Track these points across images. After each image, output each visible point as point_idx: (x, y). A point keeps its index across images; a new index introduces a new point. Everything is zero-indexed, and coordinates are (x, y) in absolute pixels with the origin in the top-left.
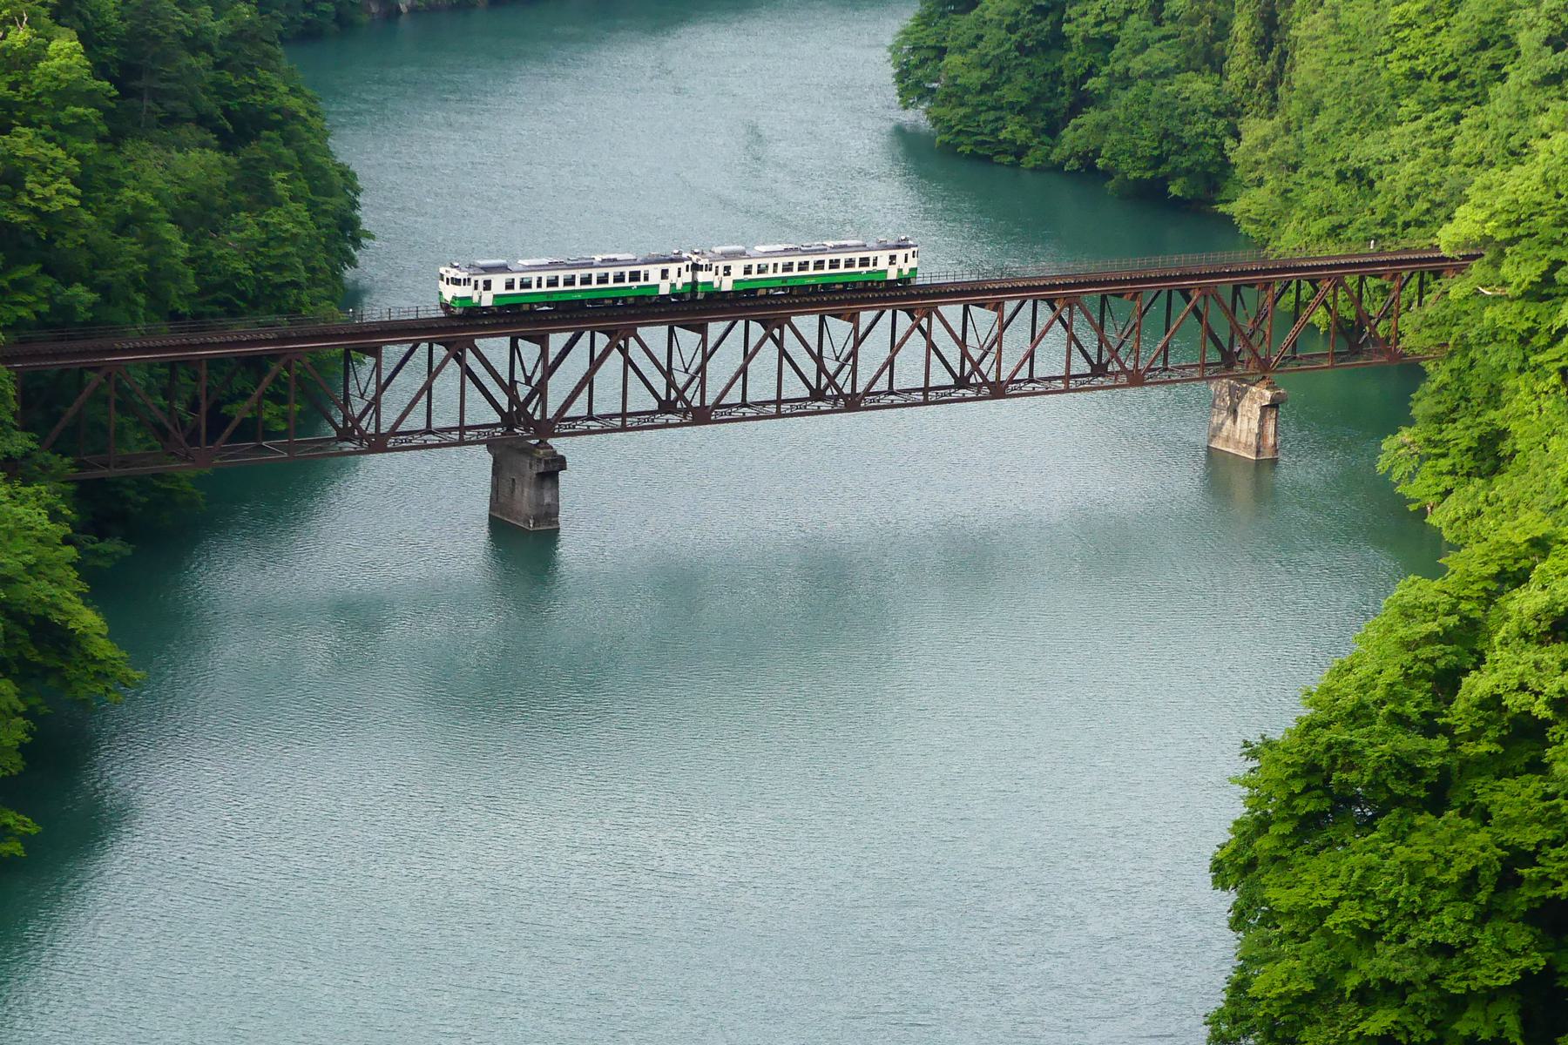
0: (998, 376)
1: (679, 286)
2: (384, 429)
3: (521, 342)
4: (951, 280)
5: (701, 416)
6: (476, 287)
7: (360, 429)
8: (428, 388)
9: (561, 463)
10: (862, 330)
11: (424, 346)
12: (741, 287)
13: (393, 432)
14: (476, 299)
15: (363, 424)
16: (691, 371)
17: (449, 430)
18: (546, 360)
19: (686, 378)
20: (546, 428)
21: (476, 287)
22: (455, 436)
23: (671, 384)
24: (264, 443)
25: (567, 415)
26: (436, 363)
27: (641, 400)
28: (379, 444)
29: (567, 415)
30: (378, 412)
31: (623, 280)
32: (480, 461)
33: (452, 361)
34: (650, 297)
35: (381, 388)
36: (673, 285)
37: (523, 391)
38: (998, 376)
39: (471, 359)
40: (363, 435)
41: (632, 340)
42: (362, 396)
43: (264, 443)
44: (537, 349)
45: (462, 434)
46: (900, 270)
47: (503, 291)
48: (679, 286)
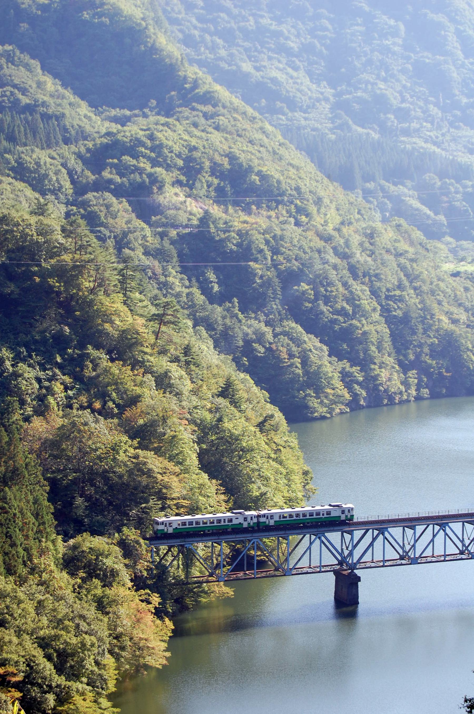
0: (415, 556)
1: (252, 524)
2: (417, 556)
3: (345, 534)
4: (397, 518)
5: (414, 561)
6: (267, 518)
7: (468, 550)
8: (432, 540)
9: (359, 579)
10: (418, 535)
11: (431, 526)
12: (177, 531)
13: (420, 557)
14: (267, 522)
15: (409, 554)
16: (471, 539)
17: (440, 556)
18: (415, 537)
19: (469, 541)
20: (353, 567)
21: (267, 518)
22: (442, 558)
23: (464, 545)
24: (247, 572)
25: (361, 561)
26: (436, 532)
27: (452, 550)
28: (287, 573)
29: (361, 561)
30: (415, 549)
31: (186, 525)
32: (331, 577)
33: (318, 539)
34: (239, 529)
35: (416, 541)
36: (249, 524)
37: (407, 548)
38: (415, 556)
39: (323, 538)
40: (409, 558)
41: (447, 527)
42: (347, 549)
43: (247, 572)
44: (350, 536)
45: (321, 569)
46: (346, 516)
47: (278, 519)
48: (252, 524)
